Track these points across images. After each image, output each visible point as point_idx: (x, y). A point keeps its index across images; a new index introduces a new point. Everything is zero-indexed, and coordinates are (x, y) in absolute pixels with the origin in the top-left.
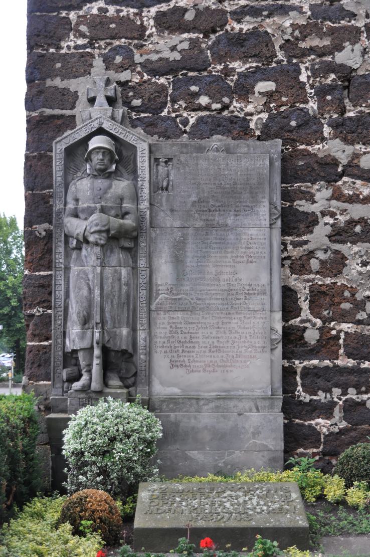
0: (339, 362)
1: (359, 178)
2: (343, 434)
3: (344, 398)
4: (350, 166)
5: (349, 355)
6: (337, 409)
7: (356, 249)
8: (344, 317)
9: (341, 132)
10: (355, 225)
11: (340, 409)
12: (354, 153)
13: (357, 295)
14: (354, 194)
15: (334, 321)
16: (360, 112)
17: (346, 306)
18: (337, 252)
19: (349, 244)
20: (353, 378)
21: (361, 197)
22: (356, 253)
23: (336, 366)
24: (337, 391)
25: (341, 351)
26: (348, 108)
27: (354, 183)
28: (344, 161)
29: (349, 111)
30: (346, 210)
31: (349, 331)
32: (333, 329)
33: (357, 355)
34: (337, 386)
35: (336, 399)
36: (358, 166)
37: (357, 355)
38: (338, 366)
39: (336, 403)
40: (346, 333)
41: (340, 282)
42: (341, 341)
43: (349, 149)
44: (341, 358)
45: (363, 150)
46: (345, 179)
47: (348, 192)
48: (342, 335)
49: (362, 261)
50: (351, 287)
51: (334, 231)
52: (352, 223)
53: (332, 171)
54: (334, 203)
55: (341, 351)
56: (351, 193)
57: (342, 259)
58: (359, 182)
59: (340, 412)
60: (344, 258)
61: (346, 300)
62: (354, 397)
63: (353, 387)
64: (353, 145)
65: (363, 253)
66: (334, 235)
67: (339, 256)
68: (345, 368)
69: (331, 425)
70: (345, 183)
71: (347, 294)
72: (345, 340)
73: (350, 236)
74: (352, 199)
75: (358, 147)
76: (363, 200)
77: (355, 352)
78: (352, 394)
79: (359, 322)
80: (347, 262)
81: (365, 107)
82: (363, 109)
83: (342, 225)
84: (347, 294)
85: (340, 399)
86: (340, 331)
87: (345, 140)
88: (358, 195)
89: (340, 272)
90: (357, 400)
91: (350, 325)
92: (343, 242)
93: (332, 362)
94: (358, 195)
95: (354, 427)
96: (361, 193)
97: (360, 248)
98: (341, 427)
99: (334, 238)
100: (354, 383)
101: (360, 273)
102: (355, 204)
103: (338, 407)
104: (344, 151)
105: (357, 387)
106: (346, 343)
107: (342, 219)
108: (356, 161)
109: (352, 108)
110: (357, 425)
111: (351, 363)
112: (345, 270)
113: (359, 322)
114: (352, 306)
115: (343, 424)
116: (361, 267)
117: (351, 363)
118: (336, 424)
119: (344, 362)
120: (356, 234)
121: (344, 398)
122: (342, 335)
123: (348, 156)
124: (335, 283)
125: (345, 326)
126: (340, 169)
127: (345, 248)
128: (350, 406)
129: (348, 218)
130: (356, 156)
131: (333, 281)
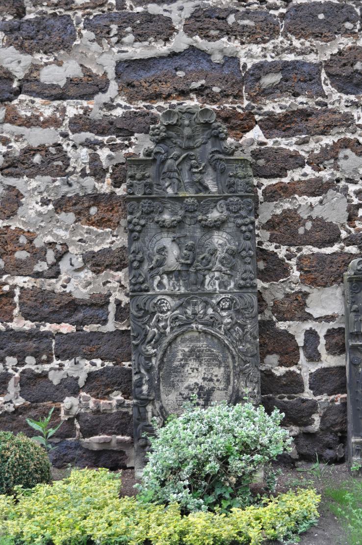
0: (13, 325)
1: (39, 95)
2: (21, 414)
3: (21, 369)
4: (28, 81)
5: (27, 316)
6: (11, 383)
7: (34, 183)
8: (19, 268)
9: (17, 38)
10: (34, 155)
11: (15, 383)
12: (33, 65)
13: (35, 242)
14: (33, 115)
15: (6, 273)
16: (43, 13)
17: (22, 255)
18: (10, 188)
19: (26, 178)
20: (32, 345)
21: (42, 119)
22: (34, 189)
23: (9, 330)
24: (11, 361)
25: (16, 311)
26: (28, 9)
27: (33, 102)
28: (20, 75)
29: (30, 12)
30: (22, 136)
31: (26, 286)
32: (5, 284)
33: (36, 315)
34: (12, 354)
35: (10, 371)
36: (37, 80)
37: (36, 315)
38: (12, 330)
39: (9, 376)
40: (22, 288)
41: (14, 225)
42: (16, 299)
43: (27, 59)
44: (15, 320)
45: (45, 60)
46: (22, 97)
47: (24, 113)
48: (17, 292)
49: (42, 199)
50: (28, 232)
51: (7, 162)
52: (29, 152)
53: (5, 87)
54: (7, 126)
55: (16, 311)
56: (29, 114)
57: (17, 196)
58: (38, 100)
59: (15, 386)
60: (19, 195)
61: (22, 248)
62: (33, 368)
63: (32, 355)
64: (31, 54)
65: (42, 189)
66: (7, 167)
67: (14, 193)
68: (20, 332)
69: (5, 403)
70: (21, 101)
71: (23, 240)
72: (20, 297)
73: (26, 168)
74: (31, 122)
75: (38, 56)
76: (43, 123)
77: (33, 312)
78: (30, 363)
79: (38, 275)
80: (23, 200)
81: (47, 6)
82: (44, 9)
83: (17, 154)
84: (23, 240)
85: (16, 371)
86: (15, 286)
87: (21, 48)
88: (37, 117)
89: (14, 213)
90: (37, 371)
91: (27, 279)
92: (18, 175)
93: (5, 325)
94: (37, 117)
95: (34, 405)
96: (42, 114)
97: (39, 183)
98: (17, 404)
99: (6, 171)
100: (32, 350)
101: (40, 214)
102: (34, 128)
103: (12, 380)
104: (19, 62)
105: (36, 355)
106: (22, 301)
107: (17, 147)
108: (35, 75)
109: (33, 9)
110: (37, 401)
111: (27, 325)
112: (20, 211)
113: (38, 275)
114: (29, 255)
115: (20, 402)
116: (42, 205)
117: (27, 325)
118: (11, 402)
119: (21, 324)
120: (34, 166)
121: (21, 369)
122: (17, 292)
123: (24, 68)
124: (8, 227)
125: (20, 281)
126: (15, 85)
127: (19, 183)
128: (29, 379)
129: (25, 145)
130: (36, 68)
131: (5, 224)
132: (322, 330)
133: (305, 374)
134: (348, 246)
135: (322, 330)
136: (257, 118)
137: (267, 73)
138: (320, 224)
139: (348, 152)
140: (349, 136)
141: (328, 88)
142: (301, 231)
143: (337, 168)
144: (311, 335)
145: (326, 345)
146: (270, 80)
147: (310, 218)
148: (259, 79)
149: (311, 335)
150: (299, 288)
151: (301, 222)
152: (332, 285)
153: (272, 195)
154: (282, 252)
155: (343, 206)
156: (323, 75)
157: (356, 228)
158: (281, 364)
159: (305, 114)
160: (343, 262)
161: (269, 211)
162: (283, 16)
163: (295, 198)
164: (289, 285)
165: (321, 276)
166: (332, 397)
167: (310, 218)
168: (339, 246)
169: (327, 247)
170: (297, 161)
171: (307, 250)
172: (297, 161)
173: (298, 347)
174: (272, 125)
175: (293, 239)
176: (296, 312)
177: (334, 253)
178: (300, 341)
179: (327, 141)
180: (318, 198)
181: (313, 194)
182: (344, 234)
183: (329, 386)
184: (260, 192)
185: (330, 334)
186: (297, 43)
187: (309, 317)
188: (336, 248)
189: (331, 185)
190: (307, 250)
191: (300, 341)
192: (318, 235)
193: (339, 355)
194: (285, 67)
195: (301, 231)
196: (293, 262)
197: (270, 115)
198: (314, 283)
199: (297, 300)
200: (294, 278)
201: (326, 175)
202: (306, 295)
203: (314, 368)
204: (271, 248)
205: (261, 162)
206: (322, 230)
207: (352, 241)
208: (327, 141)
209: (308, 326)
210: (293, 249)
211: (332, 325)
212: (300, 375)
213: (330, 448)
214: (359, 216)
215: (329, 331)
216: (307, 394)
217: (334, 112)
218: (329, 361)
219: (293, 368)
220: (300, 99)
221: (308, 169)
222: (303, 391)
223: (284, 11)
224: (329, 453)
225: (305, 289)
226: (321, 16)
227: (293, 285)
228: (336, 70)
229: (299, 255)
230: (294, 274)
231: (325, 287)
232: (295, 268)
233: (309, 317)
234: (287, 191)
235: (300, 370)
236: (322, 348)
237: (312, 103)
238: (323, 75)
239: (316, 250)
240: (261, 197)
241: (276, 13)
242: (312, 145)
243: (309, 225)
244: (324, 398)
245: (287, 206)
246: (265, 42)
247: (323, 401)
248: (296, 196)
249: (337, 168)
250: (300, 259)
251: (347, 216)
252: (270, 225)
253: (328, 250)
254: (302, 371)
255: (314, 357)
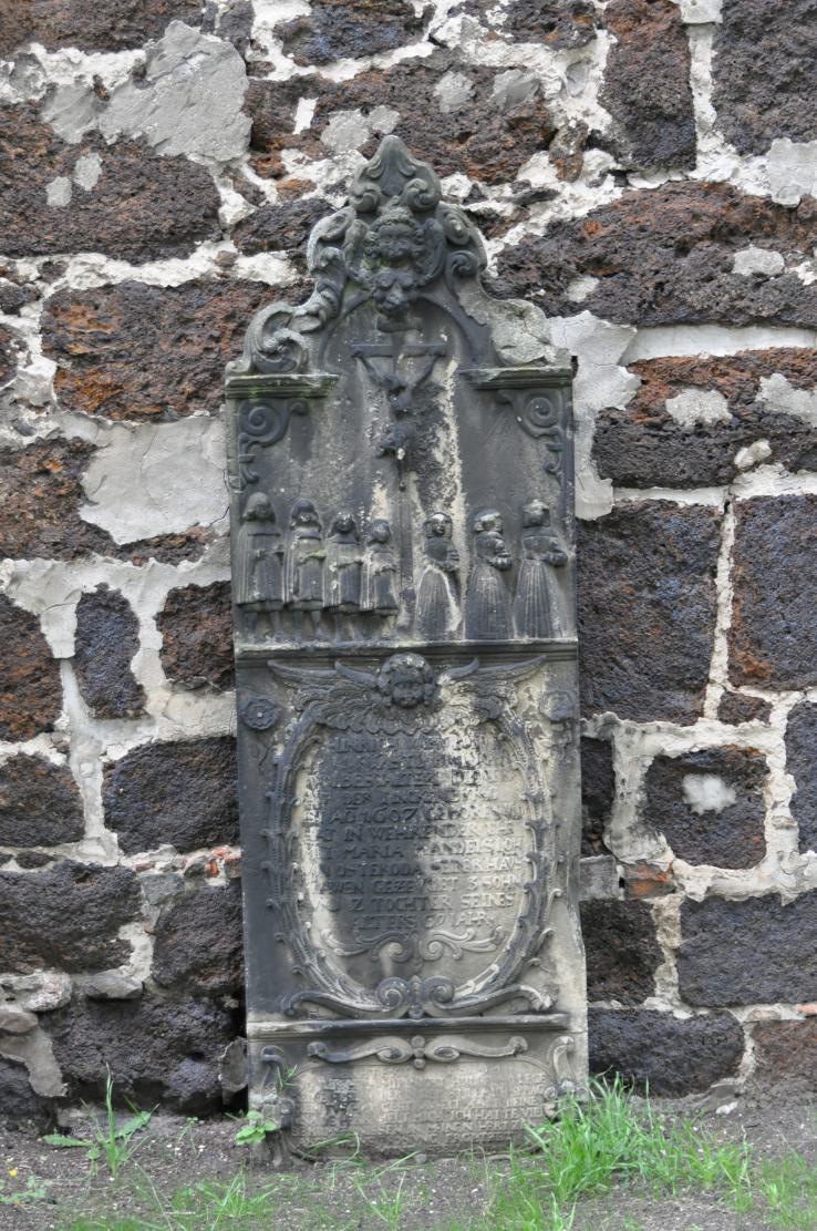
132: (147, 592)
133: (87, 768)
134: (250, 251)
135: (147, 592)
138: (134, 162)
142: (58, 193)
144: (104, 610)
145: (163, 652)
147: (93, 140)
149: (105, 614)
150: (53, 425)
151: (58, 157)
152: (184, 411)
155: (231, 87)
157: (286, 180)
160: (230, 317)
163: (32, 58)
164: (11, 415)
165: (142, 378)
166: (194, 858)
167: (93, 140)
168: (214, 254)
169: (165, 258)
171: (84, 271)
173: (54, 664)
176: (44, 524)
177: (193, 285)
178: (61, 637)
180: (128, 59)
181: (106, 42)
182: (233, 207)
183: (183, 815)
185: (179, 608)
187: (95, 542)
188: (202, 261)
190: (84, 271)
191: (61, 637)
192: (129, 211)
193: (217, 692)
195: (58, 193)
198: (112, 403)
199: (46, 472)
200: (31, 384)
202: (81, 453)
203: (119, 744)
206: (142, 188)
207: (264, 235)
209: (92, 575)
211: (187, 573)
212: (65, 770)
213: (198, 1057)
214: (297, 131)
215: (174, 596)
216: (99, 847)
218: (182, 716)
219: (35, 746)
222: (78, 835)
224: (190, 1075)
225: (79, 429)
227: (28, 416)
229: (49, 291)
230: (30, 370)
231: (157, 419)
232: (35, 343)
235: (65, 751)
236: (147, 665)
239: (119, 271)
243: (89, 170)
244: (159, 861)
247: (156, 872)
248: (37, 49)
250: (55, 307)
251: (246, 130)
253: (168, 272)
254: (75, 755)
255: (117, 700)
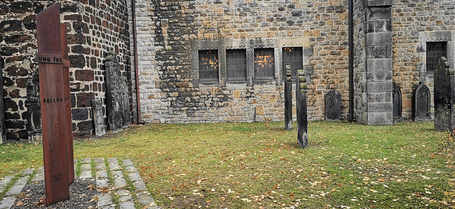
135: (24, 100)
136: (4, 38)
137: (5, 24)
138: (22, 69)
139: (30, 47)
140: (30, 42)
141: (24, 28)
142: (17, 71)
143: (27, 52)
146: (6, 26)
147: (19, 67)
148: (3, 26)
149: (21, 102)
153: (8, 61)
154: (11, 78)
156: (22, 24)
158: (12, 111)
159: (17, 36)
161: (7, 66)
162: (10, 6)
167: (19, 67)
170: (16, 50)
171: (19, 77)
172: (16, 50)
174: (8, 40)
175: (14, 74)
179: (24, 44)
182: (29, 72)
184: (5, 60)
186: (14, 15)
188: (27, 76)
189: (25, 57)
190: (19, 77)
192: (22, 73)
194: (11, 22)
195: (17, 71)
196: (15, 81)
197: (7, 36)
201: (23, 55)
202: (19, 90)
203: (22, 111)
204: (8, 76)
205: (5, 51)
208: (24, 44)
209: (20, 99)
210: (15, 77)
217: (26, 35)
220: (15, 32)
221: (19, 53)
223: (10, 4)
225: (19, 88)
226: (21, 6)
228: (26, 22)
233: (19, 97)
234: (13, 60)
236: (24, 106)
237: (19, 33)
238: (22, 24)
239: (21, 77)
240: (5, 62)
241: (8, 5)
242: (20, 45)
243: (19, 70)
245: (12, 64)
246: (5, 14)
249: (27, 52)
252: (7, 70)
